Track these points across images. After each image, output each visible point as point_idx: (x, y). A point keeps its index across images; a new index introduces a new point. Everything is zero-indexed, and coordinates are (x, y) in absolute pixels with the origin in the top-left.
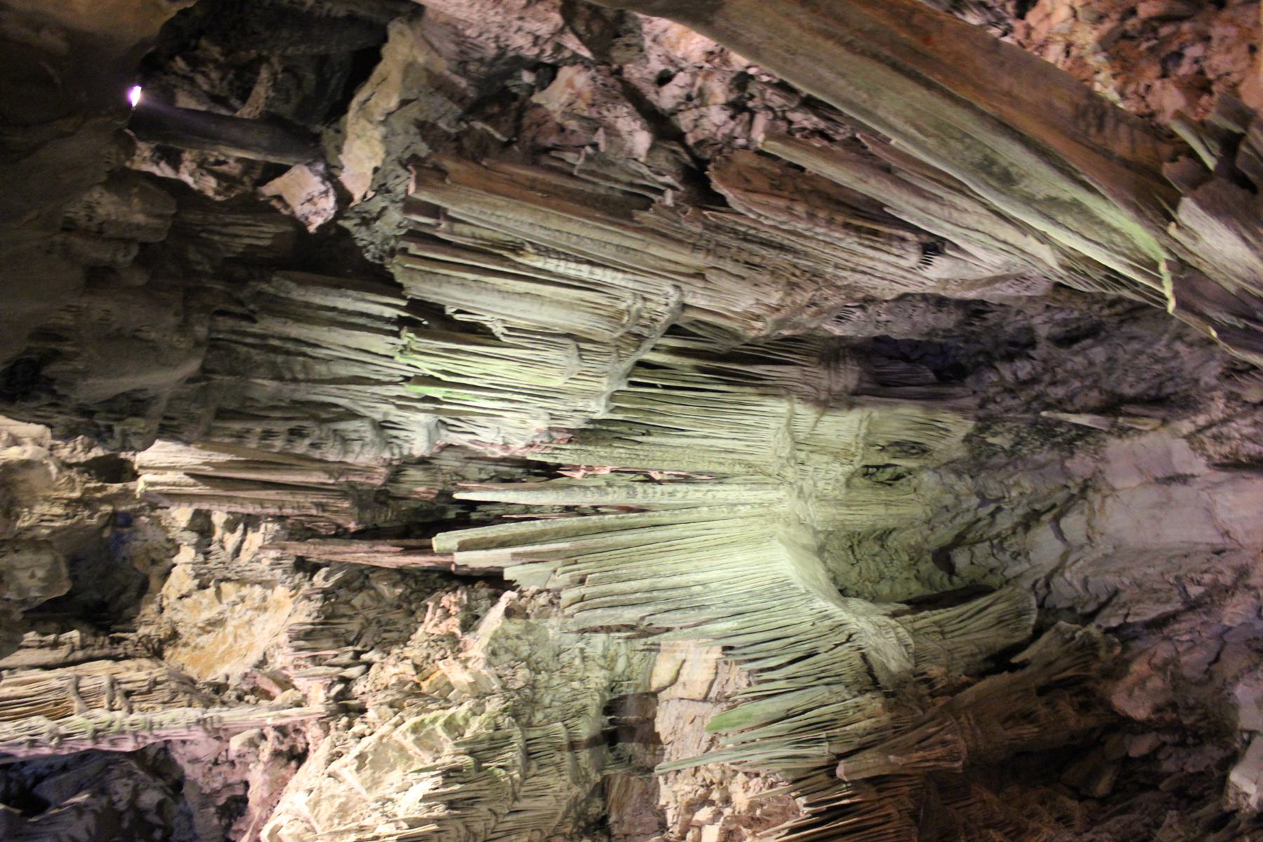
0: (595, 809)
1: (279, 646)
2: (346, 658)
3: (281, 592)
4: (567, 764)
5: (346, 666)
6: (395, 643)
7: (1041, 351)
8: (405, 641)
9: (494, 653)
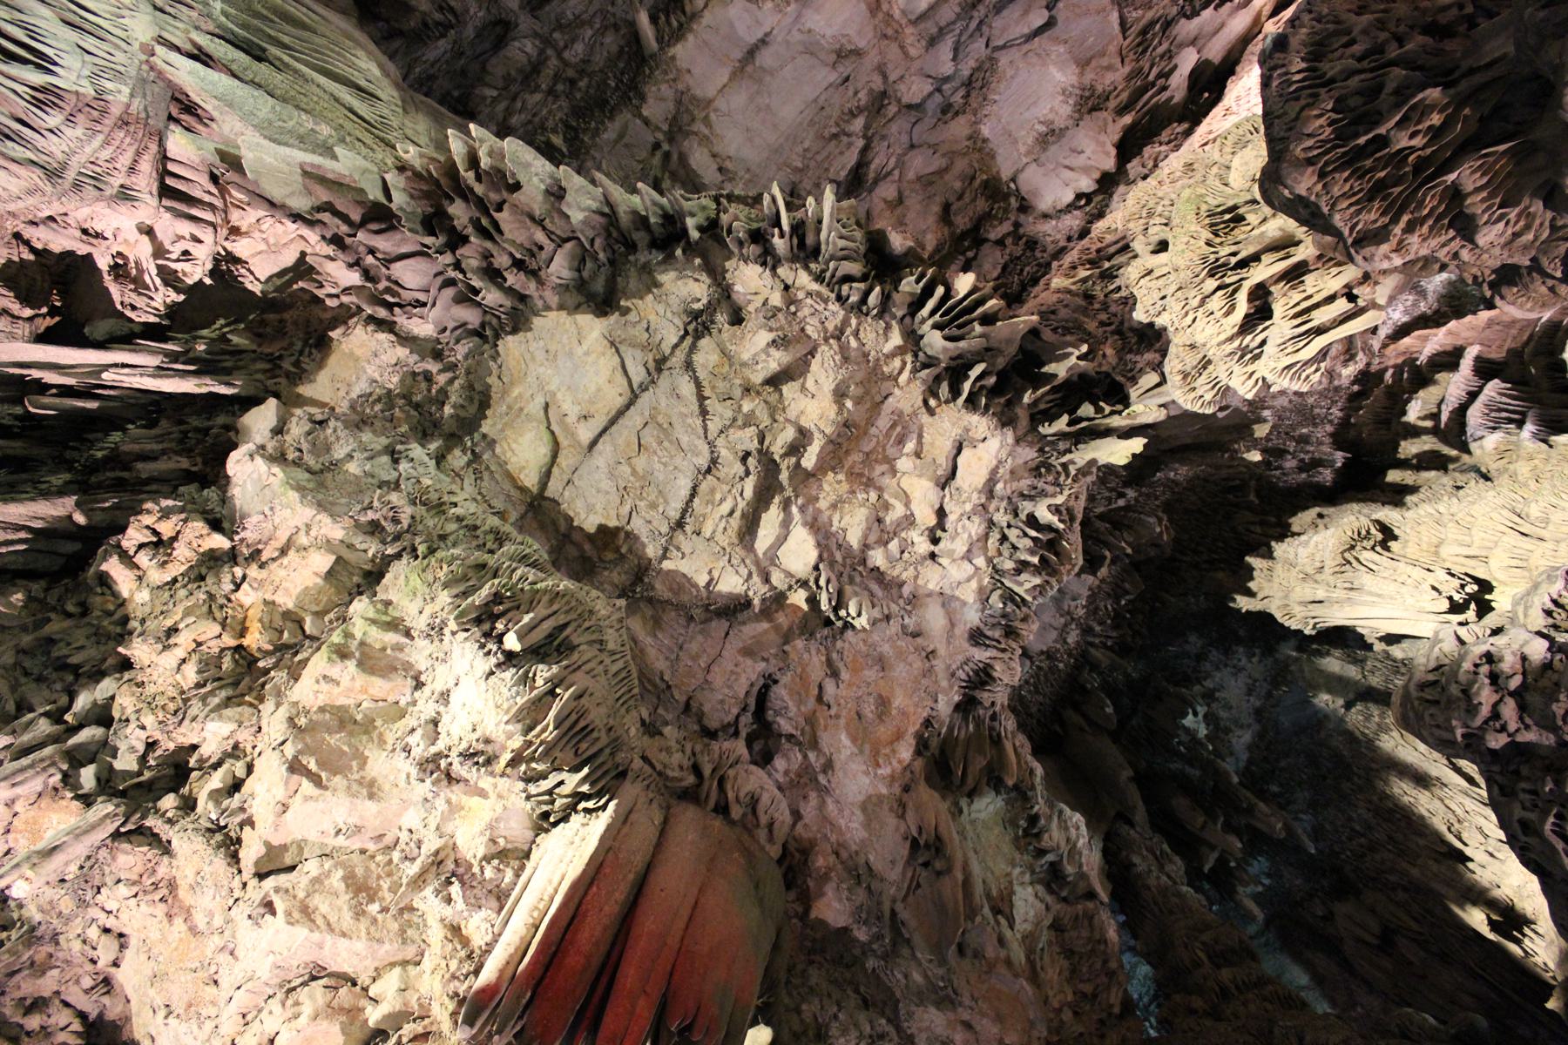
7: (525, 22)
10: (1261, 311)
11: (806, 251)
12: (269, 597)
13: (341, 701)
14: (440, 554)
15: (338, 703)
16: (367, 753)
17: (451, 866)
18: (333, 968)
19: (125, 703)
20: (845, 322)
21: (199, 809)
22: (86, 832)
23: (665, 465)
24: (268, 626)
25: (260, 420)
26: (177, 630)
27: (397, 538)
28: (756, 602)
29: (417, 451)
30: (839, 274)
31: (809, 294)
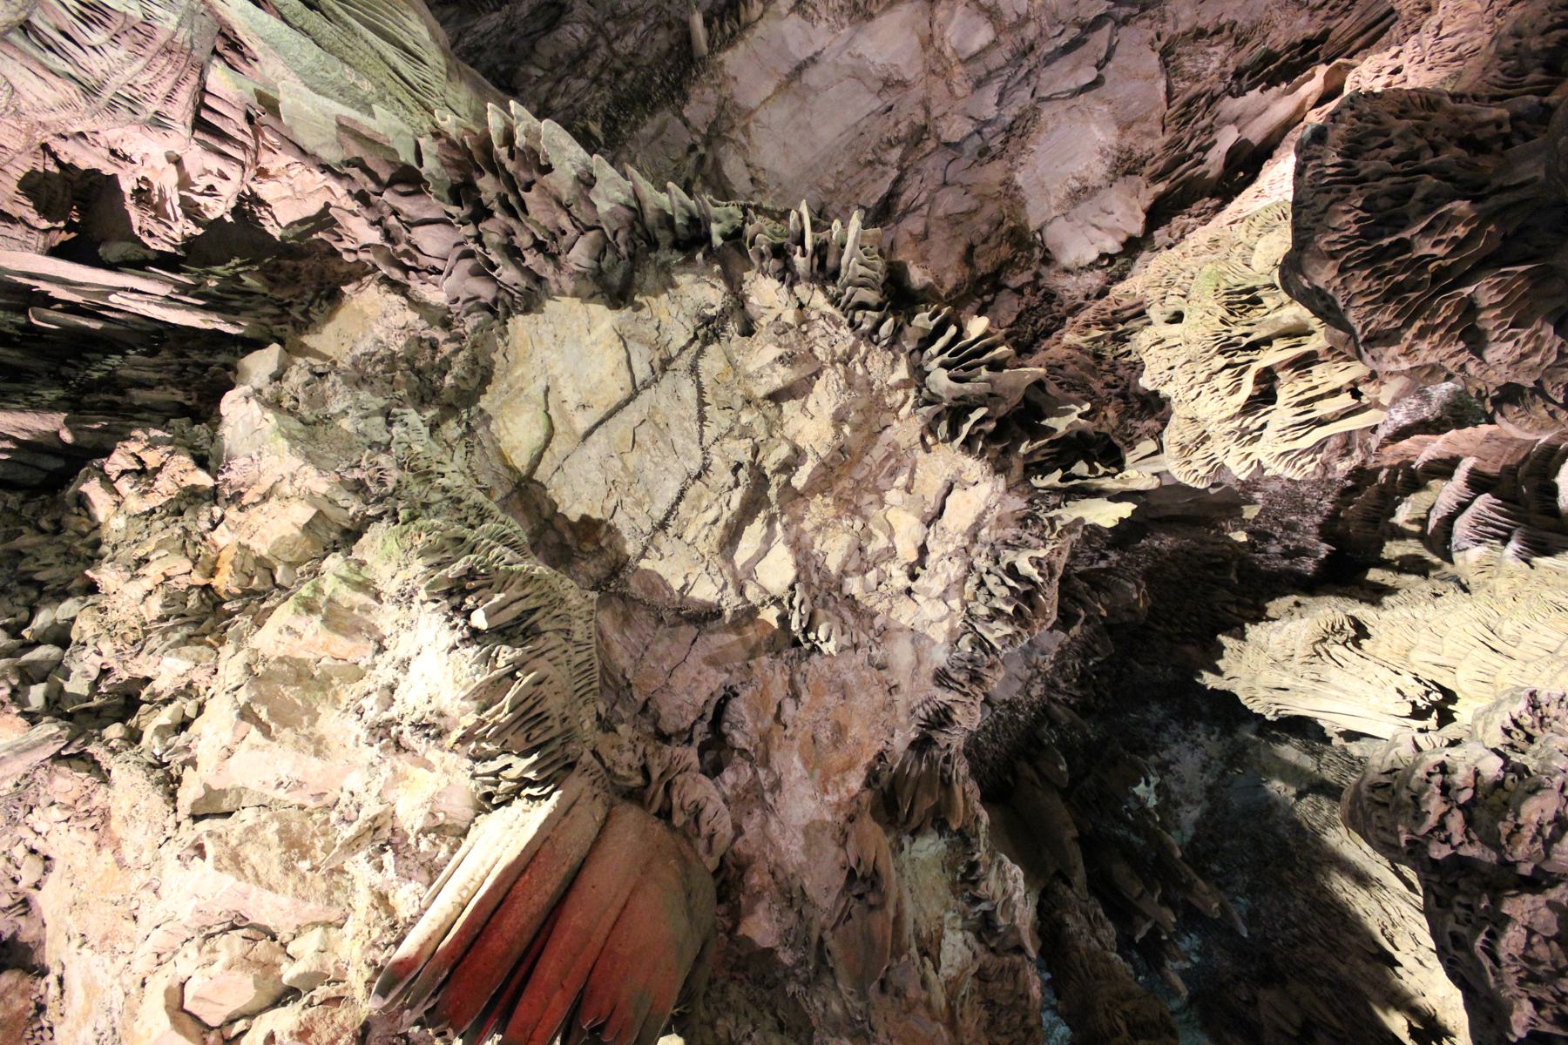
10: (1265, 395)
11: (825, 274)
12: (244, 541)
13: (301, 655)
14: (420, 522)
15: (298, 656)
16: (319, 709)
17: (387, 834)
18: (254, 920)
19: (85, 626)
20: (854, 348)
21: (144, 743)
22: (27, 750)
23: (656, 464)
24: (239, 570)
25: (261, 364)
26: (147, 561)
27: (380, 500)
28: (728, 613)
29: (412, 416)
30: (855, 300)
31: (823, 316)
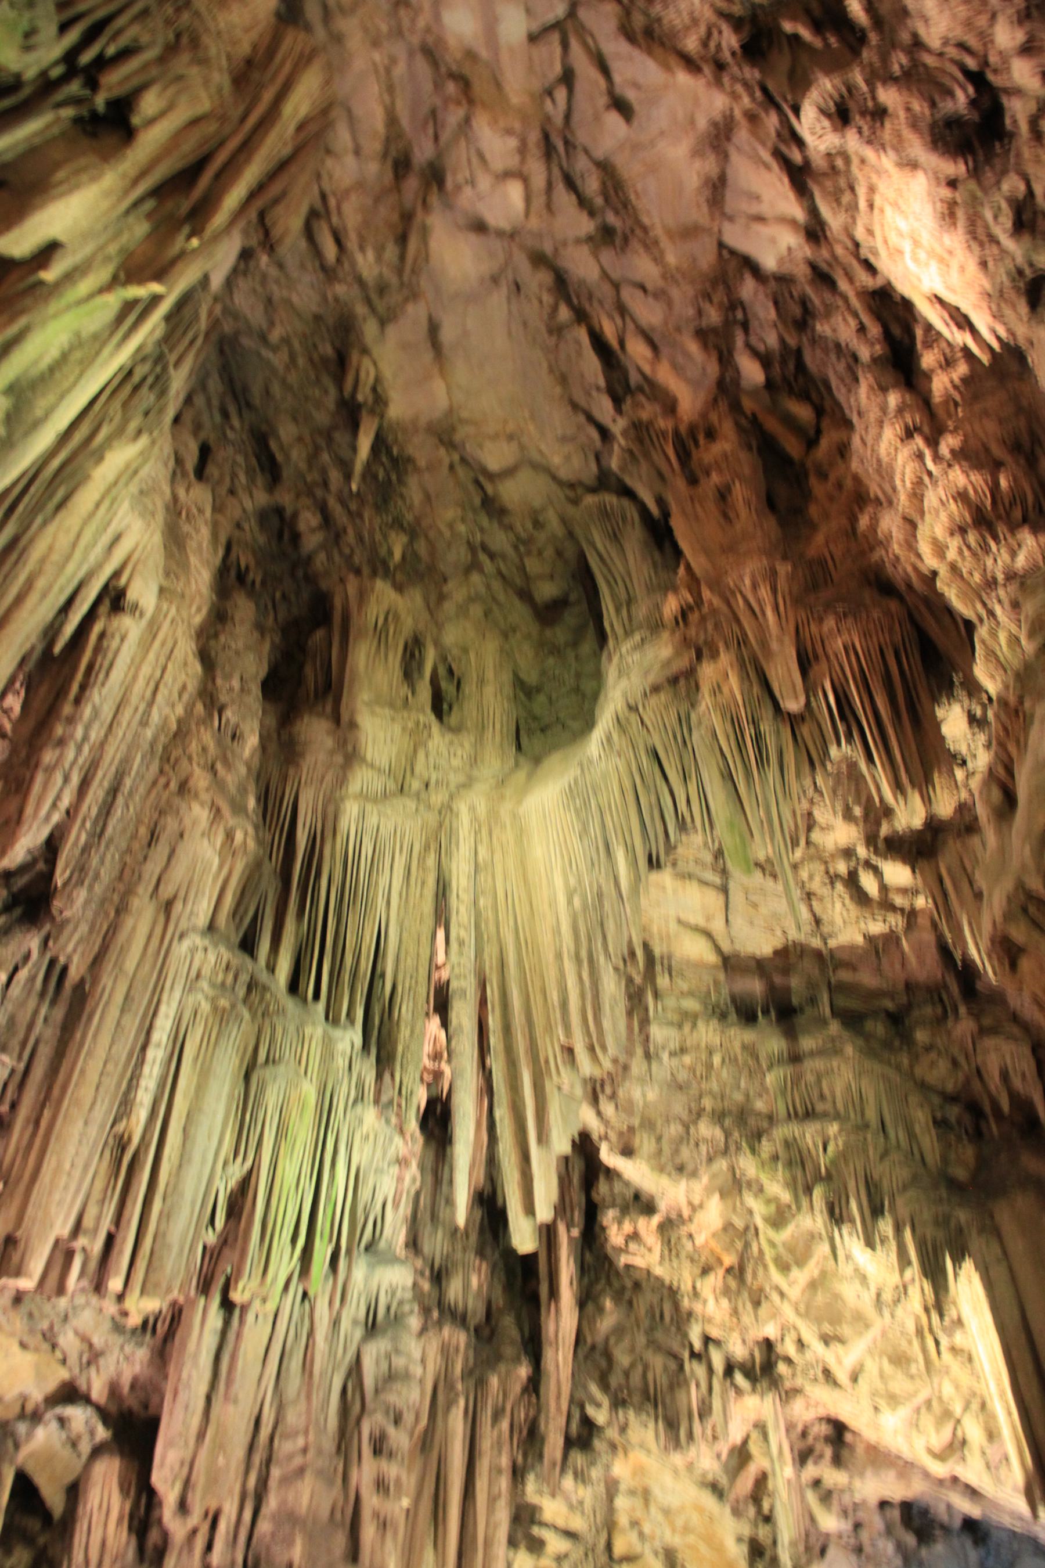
0: (878, 1028)
1: (690, 1467)
2: (699, 1370)
3: (620, 1469)
4: (818, 1064)
5: (710, 1371)
6: (676, 1306)
7: (285, 498)
8: (673, 1293)
9: (680, 1169)
